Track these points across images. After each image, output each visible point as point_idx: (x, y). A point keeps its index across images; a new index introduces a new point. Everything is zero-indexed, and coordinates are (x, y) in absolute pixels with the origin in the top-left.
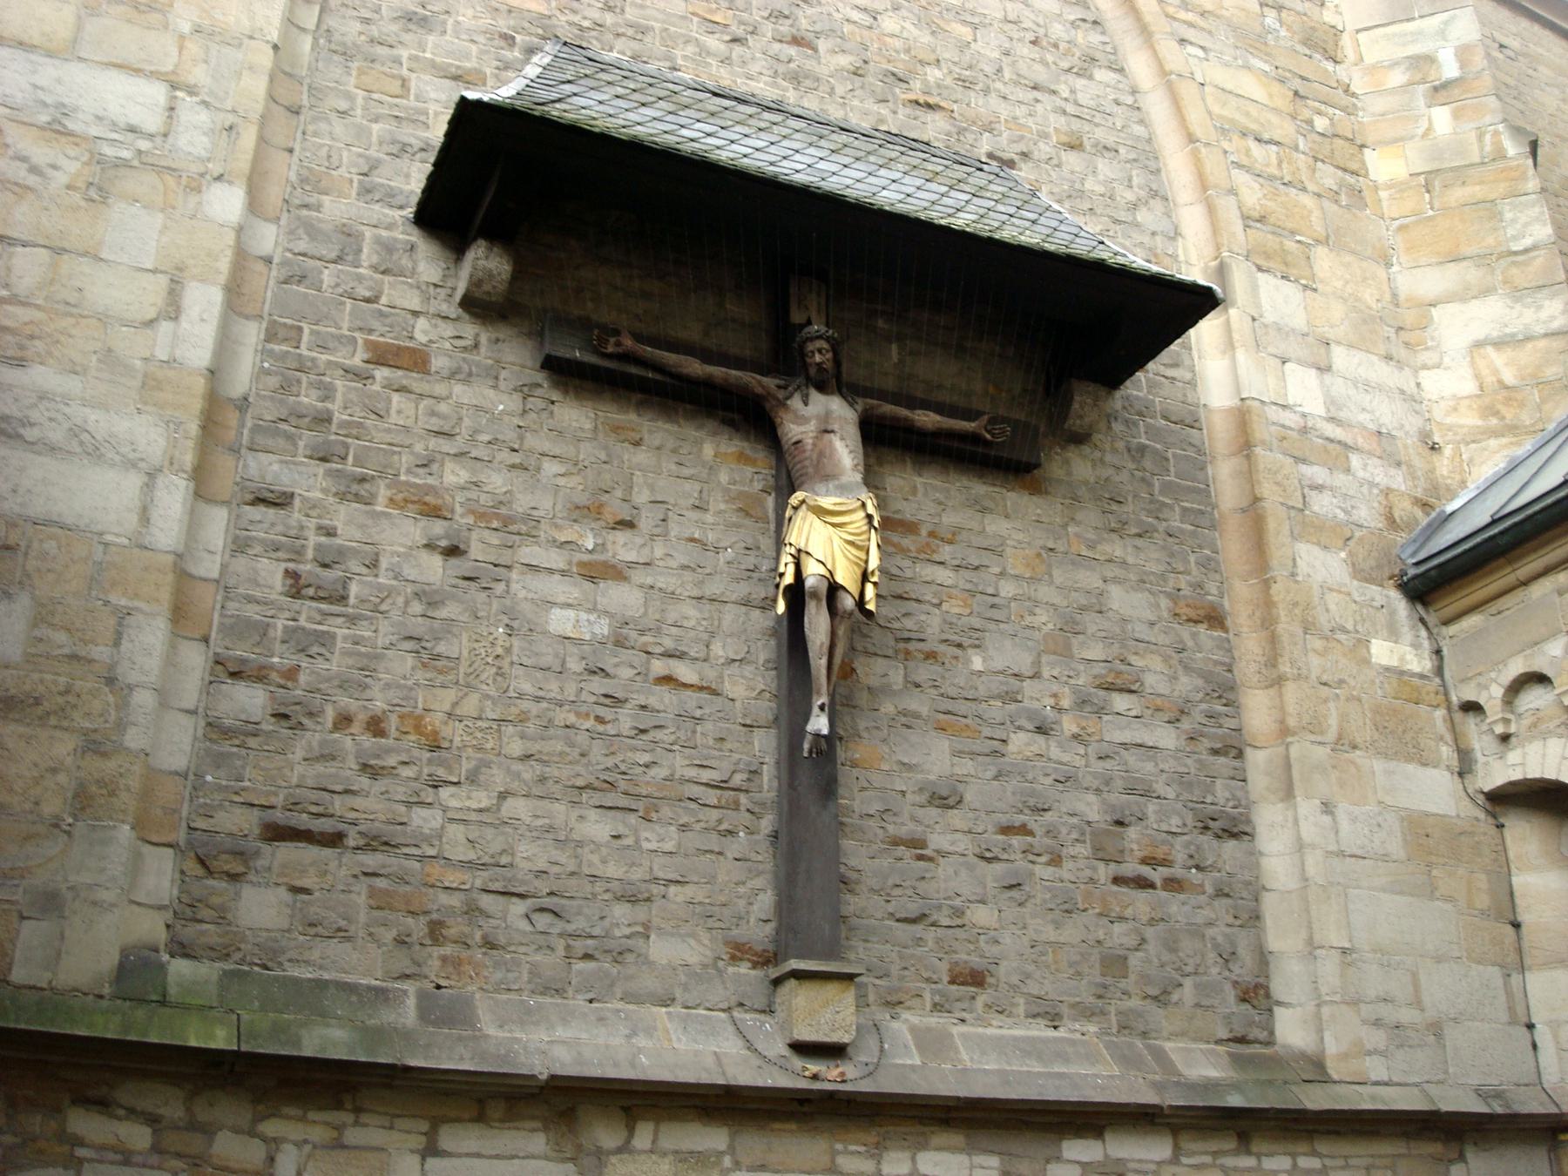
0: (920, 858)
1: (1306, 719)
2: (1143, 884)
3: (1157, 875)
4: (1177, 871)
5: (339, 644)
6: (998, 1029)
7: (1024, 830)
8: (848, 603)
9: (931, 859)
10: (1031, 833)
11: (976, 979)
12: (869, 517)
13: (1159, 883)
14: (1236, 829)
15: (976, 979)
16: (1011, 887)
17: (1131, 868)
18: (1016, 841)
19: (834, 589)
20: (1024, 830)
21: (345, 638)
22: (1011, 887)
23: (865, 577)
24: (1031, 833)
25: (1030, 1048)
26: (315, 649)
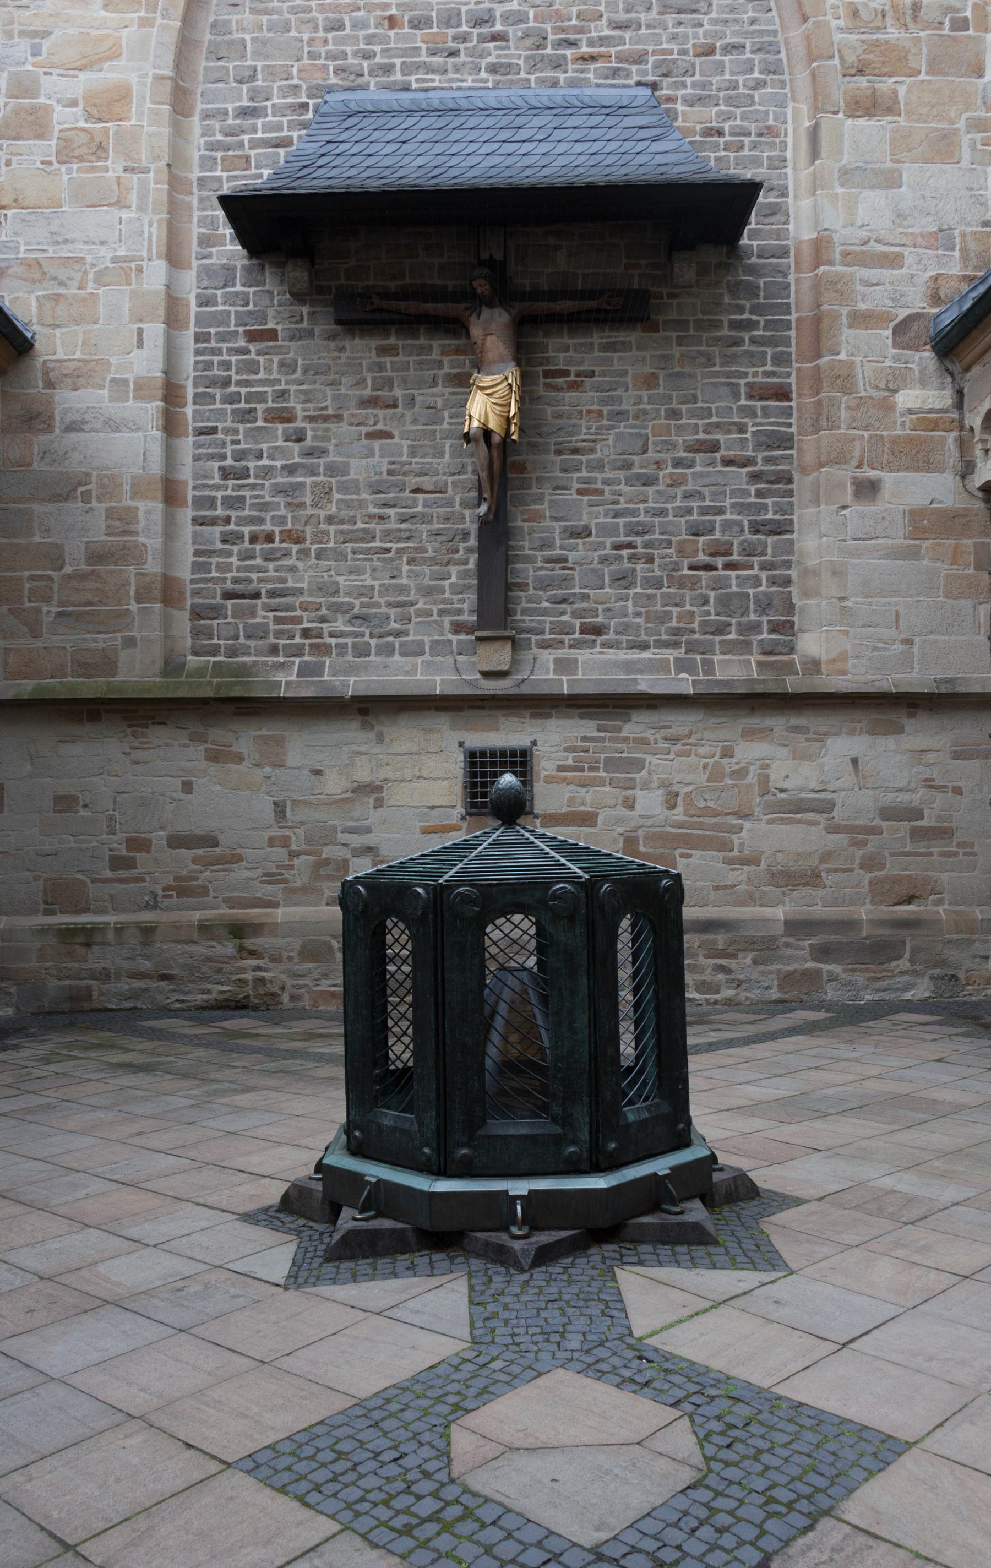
0: (563, 568)
1: (834, 454)
2: (709, 568)
3: (719, 561)
4: (735, 557)
5: (248, 501)
6: (611, 655)
7: (630, 546)
8: (496, 439)
9: (571, 569)
10: (635, 547)
11: (597, 630)
12: (510, 386)
13: (720, 566)
14: (780, 528)
15: (597, 630)
16: (619, 579)
17: (702, 558)
18: (625, 552)
19: (487, 433)
20: (630, 546)
21: (251, 497)
22: (619, 579)
23: (508, 421)
24: (635, 547)
25: (629, 666)
26: (237, 505)
